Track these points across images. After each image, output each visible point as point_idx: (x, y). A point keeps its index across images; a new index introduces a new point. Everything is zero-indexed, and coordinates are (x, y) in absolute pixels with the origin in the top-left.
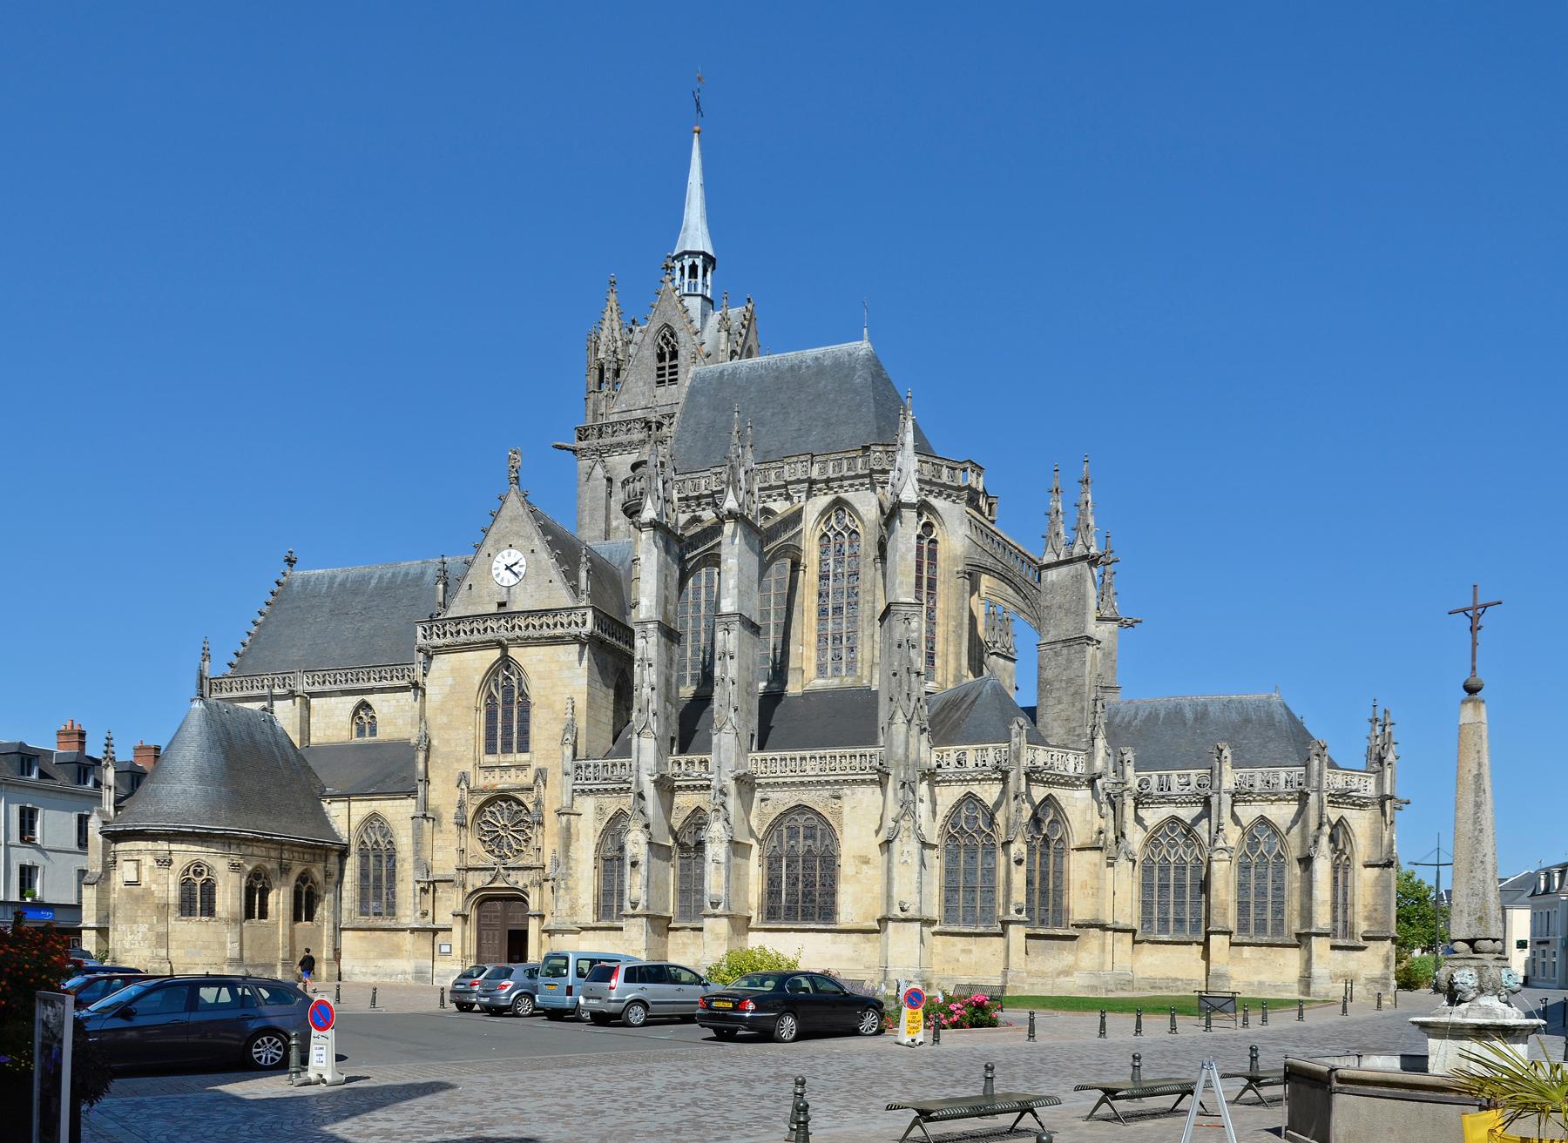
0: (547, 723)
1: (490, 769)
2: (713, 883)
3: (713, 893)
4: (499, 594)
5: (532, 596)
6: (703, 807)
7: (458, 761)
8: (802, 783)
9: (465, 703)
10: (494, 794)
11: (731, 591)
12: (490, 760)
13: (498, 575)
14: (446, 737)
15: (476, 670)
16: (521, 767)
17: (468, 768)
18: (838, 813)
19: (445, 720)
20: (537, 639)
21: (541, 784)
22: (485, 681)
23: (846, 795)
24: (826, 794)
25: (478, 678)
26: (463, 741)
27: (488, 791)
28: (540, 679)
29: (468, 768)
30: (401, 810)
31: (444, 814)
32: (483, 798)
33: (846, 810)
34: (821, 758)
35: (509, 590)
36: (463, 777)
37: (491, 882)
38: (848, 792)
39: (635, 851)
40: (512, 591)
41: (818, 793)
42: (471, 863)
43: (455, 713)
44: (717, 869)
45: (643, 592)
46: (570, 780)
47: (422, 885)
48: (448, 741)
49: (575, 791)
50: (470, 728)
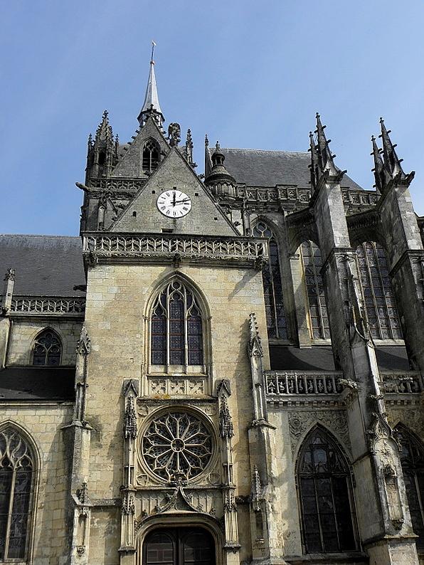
6: (404, 423)
7: (125, 368)
9: (132, 312)
15: (145, 282)
17: (136, 375)
19: (108, 326)
26: (130, 348)
31: (105, 426)
32: (153, 410)
35: (175, 221)
36: (130, 387)
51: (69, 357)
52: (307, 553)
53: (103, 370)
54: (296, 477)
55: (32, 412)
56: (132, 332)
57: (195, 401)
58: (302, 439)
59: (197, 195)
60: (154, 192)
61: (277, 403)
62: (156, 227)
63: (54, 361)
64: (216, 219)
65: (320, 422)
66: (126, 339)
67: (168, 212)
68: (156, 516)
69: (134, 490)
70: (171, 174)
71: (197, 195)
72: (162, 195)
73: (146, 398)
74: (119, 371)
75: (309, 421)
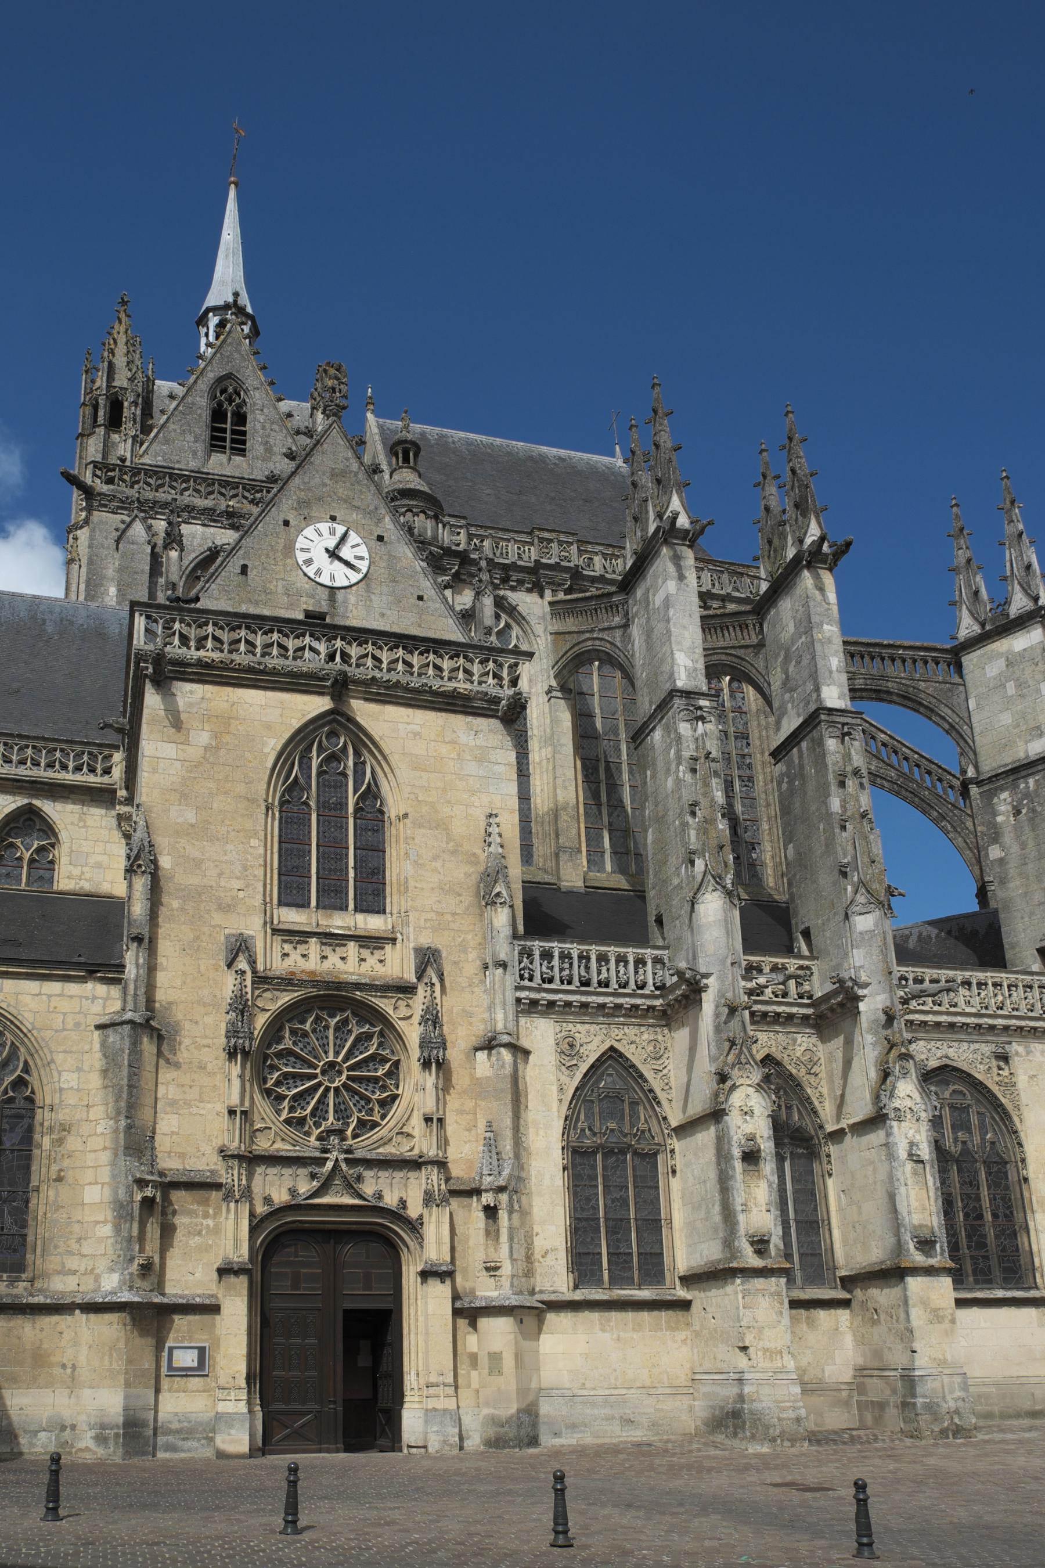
0: (435, 858)
1: (297, 936)
2: (914, 1204)
3: (916, 1222)
4: (312, 596)
5: (383, 615)
6: (778, 1056)
7: (226, 908)
8: (952, 1025)
9: (241, 789)
10: (314, 992)
11: (835, 675)
12: (292, 917)
13: (309, 562)
14: (193, 852)
15: (268, 727)
16: (371, 942)
17: (253, 927)
18: (1010, 1085)
19: (190, 816)
20: (414, 690)
21: (435, 980)
22: (285, 755)
23: (1017, 1053)
24: (987, 1049)
25: (272, 745)
26: (237, 869)
27: (302, 984)
28: (415, 769)
29: (253, 927)
30: (64, 1005)
31: (187, 1025)
32: (285, 998)
33: (1022, 1080)
34: (995, 985)
37: (316, 1194)
38: (1021, 1049)
39: (748, 1128)
40: (340, 595)
41: (973, 1046)
42: (263, 1144)
43: (215, 806)
44: (915, 1173)
45: (679, 643)
46: (510, 979)
47: (149, 1192)
48: (198, 863)
49: (518, 1000)
50: (254, 842)
51: (76, 872)
52: (576, 1287)
53: (182, 909)
54: (563, 1148)
55: (32, 986)
56: (242, 834)
57: (370, 987)
58: (579, 1076)
59: (380, 538)
60: (286, 523)
61: (534, 1003)
62: (290, 606)
63: (41, 878)
64: (420, 598)
65: (617, 1045)
66: (229, 847)
67: (319, 572)
68: (271, 1214)
69: (247, 1154)
70: (325, 485)
71: (380, 538)
72: (306, 532)
73: (270, 974)
74: (215, 915)
75: (596, 1041)
